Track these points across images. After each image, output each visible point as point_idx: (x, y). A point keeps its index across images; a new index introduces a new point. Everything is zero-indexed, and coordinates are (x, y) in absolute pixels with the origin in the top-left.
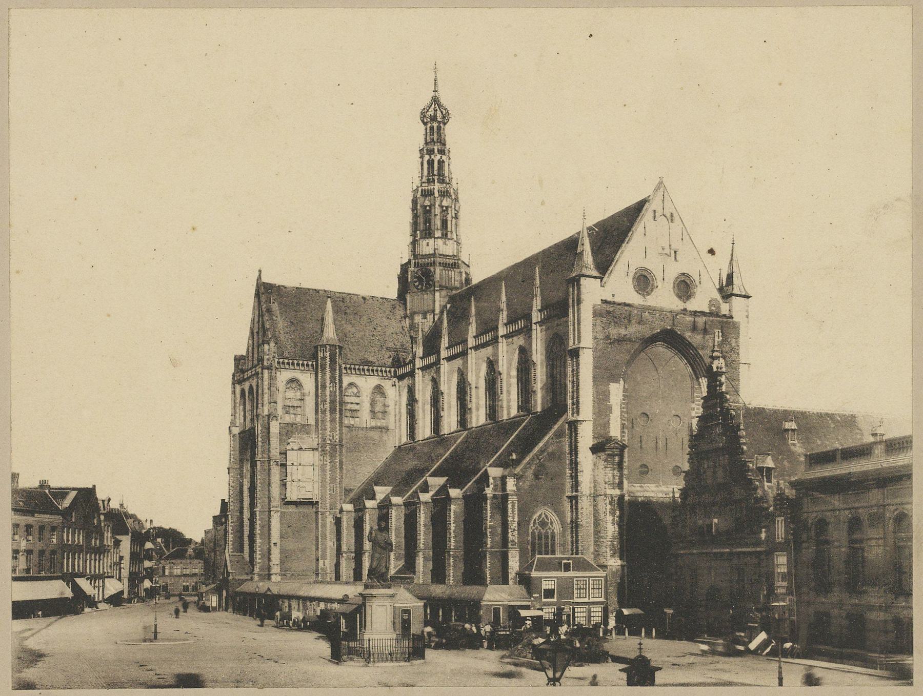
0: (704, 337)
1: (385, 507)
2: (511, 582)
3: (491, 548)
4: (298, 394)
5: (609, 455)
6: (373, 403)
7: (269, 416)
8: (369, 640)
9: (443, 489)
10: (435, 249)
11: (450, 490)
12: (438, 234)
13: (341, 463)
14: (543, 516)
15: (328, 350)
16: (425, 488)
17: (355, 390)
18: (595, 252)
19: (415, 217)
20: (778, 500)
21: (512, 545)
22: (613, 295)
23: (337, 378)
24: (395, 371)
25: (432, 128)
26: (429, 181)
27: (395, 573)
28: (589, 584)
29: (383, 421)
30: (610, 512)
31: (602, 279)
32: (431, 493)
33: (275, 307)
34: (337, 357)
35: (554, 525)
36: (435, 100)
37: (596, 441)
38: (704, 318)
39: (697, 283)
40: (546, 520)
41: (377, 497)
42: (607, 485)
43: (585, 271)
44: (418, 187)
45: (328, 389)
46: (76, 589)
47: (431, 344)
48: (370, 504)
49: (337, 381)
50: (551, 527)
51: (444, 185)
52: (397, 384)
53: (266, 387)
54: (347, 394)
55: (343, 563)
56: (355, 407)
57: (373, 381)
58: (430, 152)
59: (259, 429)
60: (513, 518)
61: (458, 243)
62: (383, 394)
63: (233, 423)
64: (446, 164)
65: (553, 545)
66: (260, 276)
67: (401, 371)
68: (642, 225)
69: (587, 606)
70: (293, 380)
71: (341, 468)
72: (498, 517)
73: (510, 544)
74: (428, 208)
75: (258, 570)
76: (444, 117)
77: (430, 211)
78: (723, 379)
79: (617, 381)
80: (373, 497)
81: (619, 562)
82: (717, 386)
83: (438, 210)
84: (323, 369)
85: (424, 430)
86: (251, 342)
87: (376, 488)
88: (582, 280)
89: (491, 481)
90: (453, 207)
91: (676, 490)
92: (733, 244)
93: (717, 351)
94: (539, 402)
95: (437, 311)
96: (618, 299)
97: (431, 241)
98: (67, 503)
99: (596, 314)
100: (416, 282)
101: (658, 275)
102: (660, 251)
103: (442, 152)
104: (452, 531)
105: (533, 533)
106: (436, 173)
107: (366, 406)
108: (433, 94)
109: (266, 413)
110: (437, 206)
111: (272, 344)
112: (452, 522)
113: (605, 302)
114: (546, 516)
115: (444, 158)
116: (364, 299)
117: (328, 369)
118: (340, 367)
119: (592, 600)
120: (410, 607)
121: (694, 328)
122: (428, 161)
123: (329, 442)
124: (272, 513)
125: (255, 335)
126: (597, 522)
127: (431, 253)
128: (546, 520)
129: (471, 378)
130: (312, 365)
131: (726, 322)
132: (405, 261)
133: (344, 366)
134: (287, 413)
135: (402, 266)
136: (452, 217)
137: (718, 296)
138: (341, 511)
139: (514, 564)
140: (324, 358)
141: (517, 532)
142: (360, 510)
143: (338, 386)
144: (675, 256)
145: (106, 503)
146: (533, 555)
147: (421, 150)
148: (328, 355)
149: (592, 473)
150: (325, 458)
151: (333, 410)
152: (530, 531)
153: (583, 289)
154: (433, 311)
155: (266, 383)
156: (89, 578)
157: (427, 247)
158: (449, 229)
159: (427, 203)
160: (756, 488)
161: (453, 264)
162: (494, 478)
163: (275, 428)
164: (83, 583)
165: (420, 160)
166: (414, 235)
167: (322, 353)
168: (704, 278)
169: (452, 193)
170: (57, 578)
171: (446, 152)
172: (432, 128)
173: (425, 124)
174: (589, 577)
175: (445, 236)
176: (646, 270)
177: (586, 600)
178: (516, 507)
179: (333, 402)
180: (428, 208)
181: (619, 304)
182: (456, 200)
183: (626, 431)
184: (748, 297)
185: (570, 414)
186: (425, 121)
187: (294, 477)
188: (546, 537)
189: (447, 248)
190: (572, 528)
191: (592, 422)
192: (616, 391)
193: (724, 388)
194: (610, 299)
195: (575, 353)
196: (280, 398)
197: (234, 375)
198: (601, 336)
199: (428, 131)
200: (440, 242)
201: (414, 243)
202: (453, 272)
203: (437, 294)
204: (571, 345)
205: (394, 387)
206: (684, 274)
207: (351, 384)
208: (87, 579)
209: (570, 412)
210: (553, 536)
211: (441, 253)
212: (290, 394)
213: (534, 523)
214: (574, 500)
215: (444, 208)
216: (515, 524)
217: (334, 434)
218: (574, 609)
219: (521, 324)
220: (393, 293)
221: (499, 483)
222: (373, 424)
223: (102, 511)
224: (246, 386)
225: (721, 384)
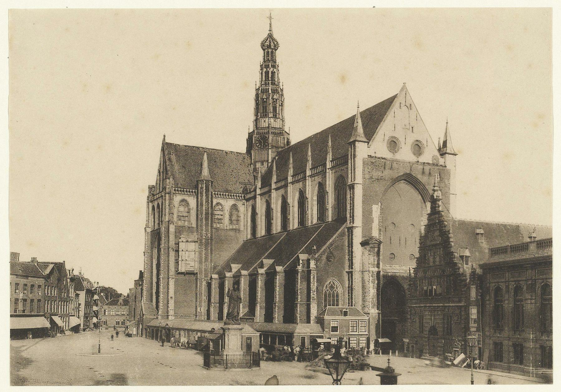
0: (429, 178)
1: (237, 278)
2: (312, 322)
3: (301, 301)
4: (186, 209)
5: (371, 247)
6: (231, 215)
7: (169, 221)
8: (227, 355)
9: (272, 267)
10: (269, 124)
11: (276, 267)
12: (271, 115)
13: (211, 249)
14: (332, 283)
15: (204, 183)
16: (262, 266)
18: (365, 127)
19: (257, 104)
20: (472, 275)
21: (313, 300)
22: (375, 153)
23: (210, 200)
24: (244, 196)
25: (268, 52)
26: (266, 84)
27: (243, 316)
28: (359, 324)
29: (237, 226)
30: (372, 281)
31: (368, 143)
32: (265, 269)
33: (173, 157)
34: (210, 187)
35: (338, 289)
36: (270, 36)
37: (364, 239)
38: (429, 167)
39: (425, 146)
40: (333, 285)
41: (233, 270)
42: (370, 265)
43: (358, 138)
44: (259, 87)
45: (204, 206)
46: (52, 322)
47: (266, 181)
48: (228, 274)
49: (210, 202)
50: (336, 289)
51: (275, 86)
52: (245, 204)
53: (167, 204)
54: (215, 209)
55: (212, 310)
56: (220, 217)
57: (231, 202)
58: (267, 67)
59: (163, 229)
61: (283, 121)
62: (237, 210)
63: (147, 226)
64: (276, 74)
65: (337, 301)
66: (164, 138)
67: (248, 196)
68: (393, 110)
69: (357, 337)
70: (183, 200)
71: (211, 253)
72: (305, 284)
73: (311, 300)
74: (265, 100)
75: (161, 313)
76: (275, 46)
77: (266, 101)
78: (440, 203)
80: (230, 271)
81: (377, 311)
82: (436, 207)
83: (271, 101)
84: (201, 193)
85: (261, 231)
86: (158, 178)
87: (233, 265)
88: (357, 143)
89: (301, 262)
90: (280, 99)
91: (411, 269)
92: (447, 123)
93: (437, 186)
94: (330, 216)
95: (270, 161)
96: (378, 155)
97: (267, 120)
98: (48, 271)
100: (257, 143)
102: (404, 126)
103: (274, 66)
104: (277, 291)
105: (326, 292)
106: (270, 79)
107: (227, 216)
108: (269, 32)
109: (167, 220)
111: (171, 179)
112: (277, 286)
113: (370, 156)
114: (334, 283)
115: (275, 70)
116: (226, 153)
117: (204, 194)
118: (212, 193)
119: (360, 333)
120: (251, 336)
122: (266, 72)
123: (204, 237)
124: (170, 279)
125: (161, 174)
126: (364, 287)
127: (266, 126)
128: (333, 285)
129: (290, 200)
130: (195, 192)
131: (442, 170)
132: (251, 130)
133: (214, 192)
134: (180, 220)
135: (249, 134)
136: (280, 105)
137: (437, 154)
138: (211, 278)
139: (314, 312)
140: (202, 188)
141: (316, 292)
142: (222, 278)
143: (210, 204)
144: (412, 129)
145: (71, 271)
146: (325, 306)
147: (261, 66)
148: (205, 186)
149: (361, 258)
150: (202, 247)
151: (207, 219)
152: (324, 292)
153: (357, 149)
154: (268, 161)
155: (167, 202)
156: (60, 316)
157: (264, 123)
158: (278, 112)
160: (459, 269)
161: (280, 132)
163: (172, 229)
164: (57, 319)
165: (261, 71)
166: (256, 115)
168: (430, 143)
169: (279, 91)
170: (41, 316)
171: (276, 66)
172: (268, 52)
173: (264, 50)
174: (359, 320)
175: (275, 117)
176: (395, 138)
177: (357, 333)
178: (316, 278)
179: (207, 214)
180: (265, 100)
181: (379, 158)
182: (282, 95)
183: (382, 233)
185: (349, 223)
186: (264, 48)
187: (183, 258)
188: (333, 296)
189: (276, 124)
190: (349, 290)
191: (362, 228)
192: (376, 210)
193: (440, 209)
194: (373, 155)
195: (352, 187)
196: (175, 211)
197: (148, 197)
198: (367, 176)
199: (266, 54)
200: (272, 120)
201: (256, 120)
202: (280, 138)
203: (270, 151)
204: (350, 182)
205: (243, 206)
206: (417, 141)
207: (218, 204)
208: (59, 317)
209: (348, 222)
210: (337, 296)
211: (273, 126)
212: (182, 209)
213: (326, 287)
214: (350, 274)
215: (275, 100)
216: (315, 288)
217: (208, 233)
218: (349, 338)
219: (320, 169)
220: (244, 151)
221: (305, 262)
222: (231, 227)
223: (69, 276)
224: (156, 204)
225: (439, 207)
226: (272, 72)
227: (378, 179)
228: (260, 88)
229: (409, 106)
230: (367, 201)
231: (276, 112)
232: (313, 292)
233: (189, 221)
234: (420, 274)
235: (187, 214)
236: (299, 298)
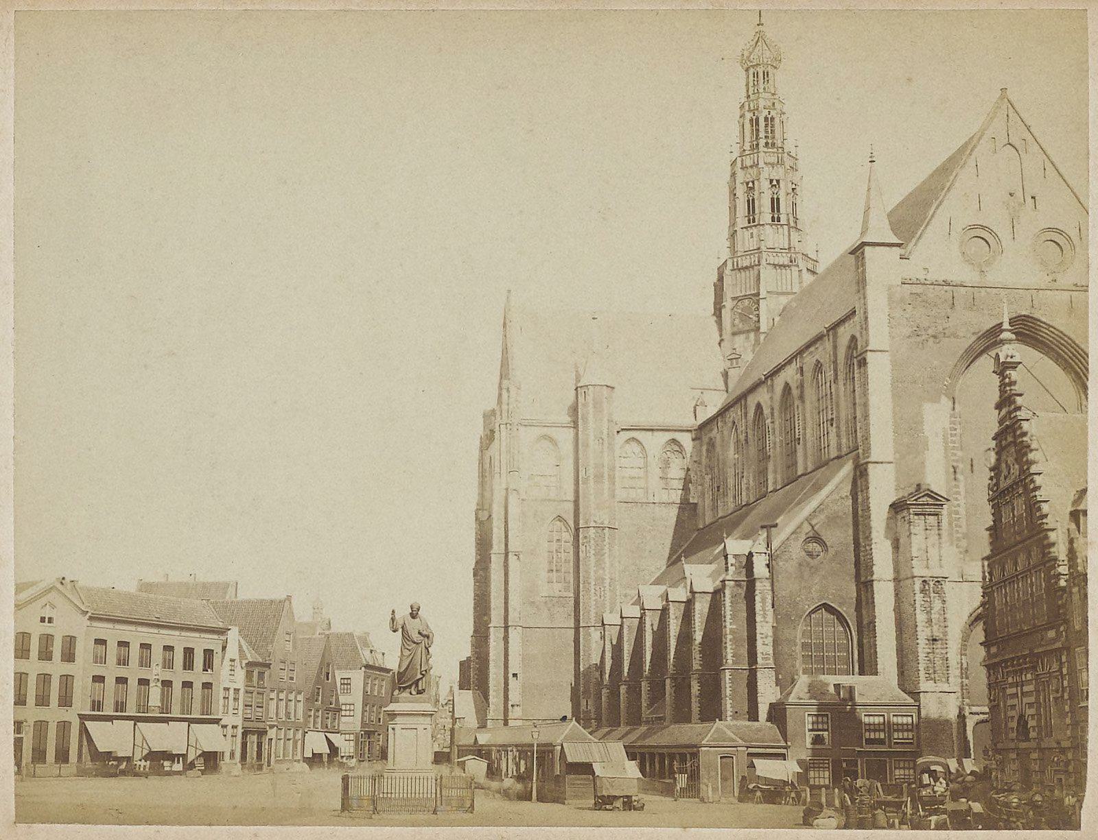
12: (767, 218)
56: (634, 473)
64: (777, 121)
74: (751, 185)
79: (935, 400)
88: (867, 249)
89: (731, 560)
101: (1004, 233)
107: (656, 472)
122: (751, 120)
124: (510, 629)
150: (588, 548)
162: (735, 556)
163: (514, 510)
176: (983, 227)
180: (751, 185)
201: (733, 235)
215: (775, 183)
226: (766, 119)
228: (739, 160)
231: (778, 211)
232: (762, 638)
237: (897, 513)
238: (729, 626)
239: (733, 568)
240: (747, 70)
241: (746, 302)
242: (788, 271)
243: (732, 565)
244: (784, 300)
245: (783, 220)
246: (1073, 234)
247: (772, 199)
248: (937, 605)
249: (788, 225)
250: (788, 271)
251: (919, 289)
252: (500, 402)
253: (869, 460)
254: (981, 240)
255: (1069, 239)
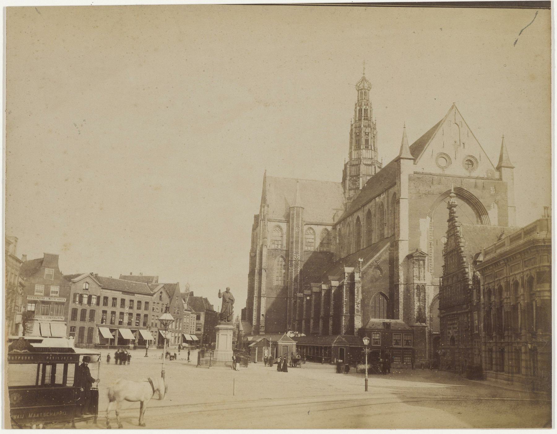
0: (483, 192)
15: (295, 210)
17: (312, 231)
30: (416, 294)
38: (483, 181)
45: (295, 230)
56: (311, 240)
60: (358, 296)
64: (369, 111)
73: (355, 312)
74: (358, 134)
83: (363, 134)
89: (346, 275)
99: (410, 179)
101: (452, 156)
108: (363, 75)
110: (362, 132)
121: (476, 186)
122: (359, 110)
134: (273, 244)
136: (371, 138)
140: (293, 214)
141: (360, 305)
147: (356, 105)
159: (357, 131)
162: (348, 273)
163: (265, 253)
166: (351, 148)
167: (292, 212)
175: (367, 148)
176: (444, 154)
182: (375, 129)
184: (513, 168)
194: (421, 171)
206: (470, 156)
215: (367, 133)
226: (365, 109)
227: (425, 194)
229: (458, 123)
230: (415, 215)
231: (368, 144)
233: (282, 245)
234: (445, 283)
235: (280, 239)
236: (344, 310)
237: (408, 259)
238: (344, 299)
239: (347, 278)
240: (358, 91)
241: (355, 178)
242: (371, 167)
243: (347, 277)
244: (369, 178)
245: (370, 147)
246: (477, 157)
247: (366, 140)
248: (422, 294)
249: (371, 149)
250: (371, 167)
251: (421, 176)
252: (261, 212)
253: (399, 239)
254: (444, 159)
255: (476, 160)
